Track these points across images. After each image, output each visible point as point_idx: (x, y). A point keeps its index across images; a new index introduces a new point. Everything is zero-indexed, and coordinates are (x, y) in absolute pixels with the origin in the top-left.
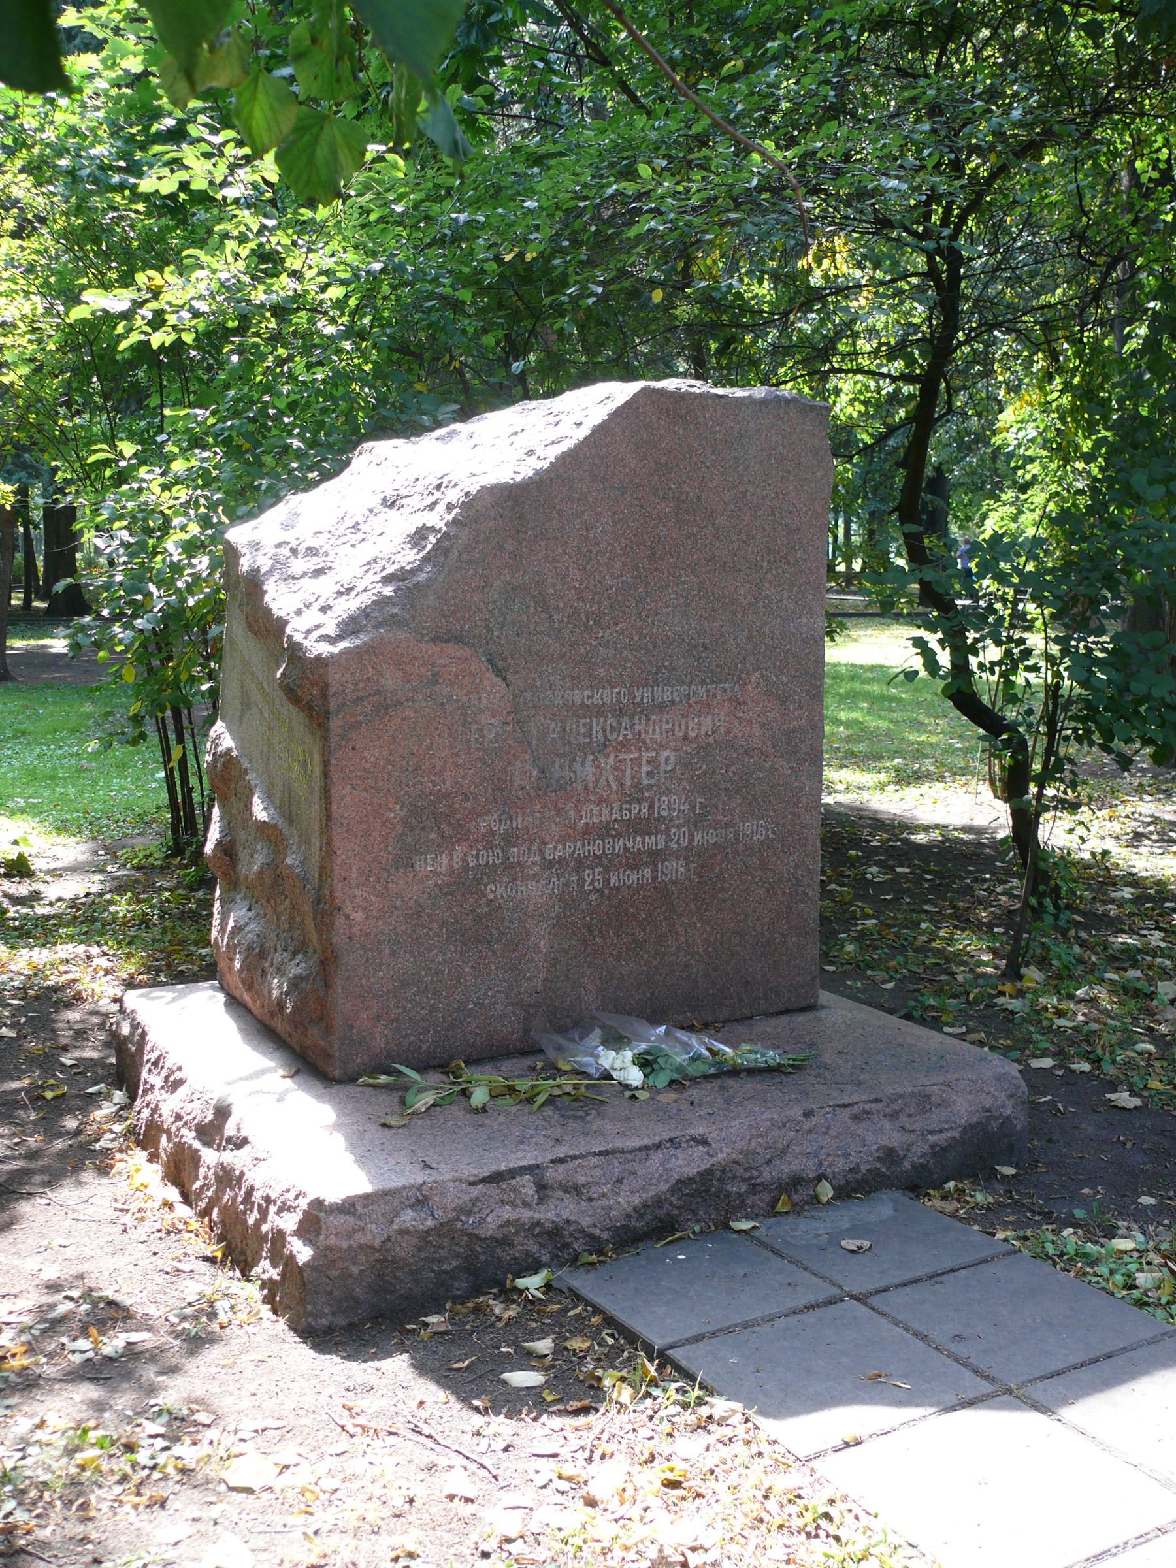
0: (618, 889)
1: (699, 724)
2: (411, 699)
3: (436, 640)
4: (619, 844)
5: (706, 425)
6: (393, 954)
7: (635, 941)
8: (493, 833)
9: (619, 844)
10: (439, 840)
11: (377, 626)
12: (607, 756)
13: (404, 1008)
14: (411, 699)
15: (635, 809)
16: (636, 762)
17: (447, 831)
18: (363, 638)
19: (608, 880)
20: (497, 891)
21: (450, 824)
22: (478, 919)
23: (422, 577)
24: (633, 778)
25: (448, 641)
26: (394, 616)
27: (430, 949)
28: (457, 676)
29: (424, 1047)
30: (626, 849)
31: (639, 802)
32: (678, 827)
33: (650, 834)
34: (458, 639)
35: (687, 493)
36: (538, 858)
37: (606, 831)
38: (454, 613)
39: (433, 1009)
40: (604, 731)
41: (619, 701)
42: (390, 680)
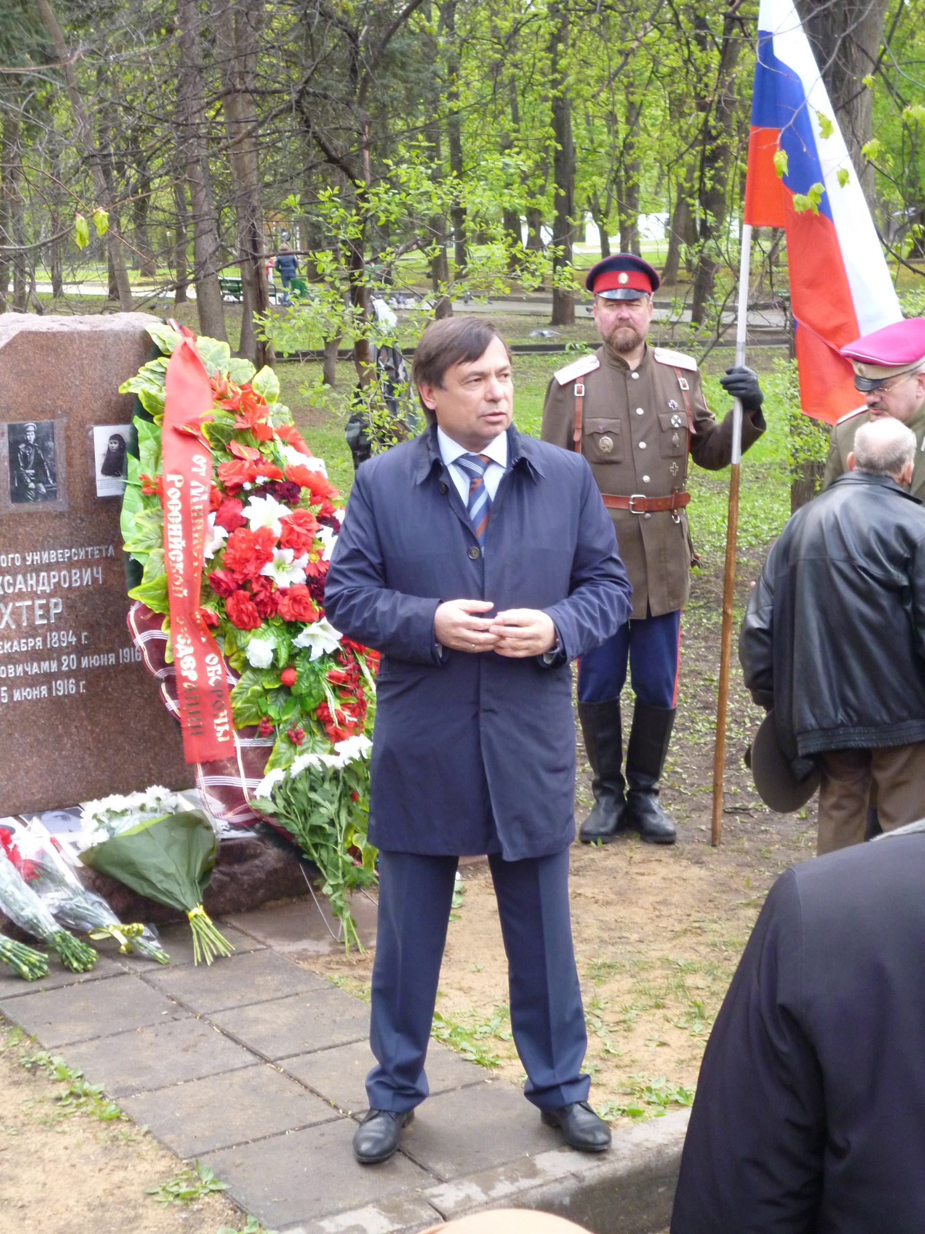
0: (20, 702)
1: (81, 577)
4: (20, 670)
7: (37, 740)
9: (20, 670)
12: (6, 606)
16: (31, 609)
19: (11, 697)
24: (28, 619)
30: (26, 672)
31: (34, 637)
33: (44, 660)
41: (13, 563)
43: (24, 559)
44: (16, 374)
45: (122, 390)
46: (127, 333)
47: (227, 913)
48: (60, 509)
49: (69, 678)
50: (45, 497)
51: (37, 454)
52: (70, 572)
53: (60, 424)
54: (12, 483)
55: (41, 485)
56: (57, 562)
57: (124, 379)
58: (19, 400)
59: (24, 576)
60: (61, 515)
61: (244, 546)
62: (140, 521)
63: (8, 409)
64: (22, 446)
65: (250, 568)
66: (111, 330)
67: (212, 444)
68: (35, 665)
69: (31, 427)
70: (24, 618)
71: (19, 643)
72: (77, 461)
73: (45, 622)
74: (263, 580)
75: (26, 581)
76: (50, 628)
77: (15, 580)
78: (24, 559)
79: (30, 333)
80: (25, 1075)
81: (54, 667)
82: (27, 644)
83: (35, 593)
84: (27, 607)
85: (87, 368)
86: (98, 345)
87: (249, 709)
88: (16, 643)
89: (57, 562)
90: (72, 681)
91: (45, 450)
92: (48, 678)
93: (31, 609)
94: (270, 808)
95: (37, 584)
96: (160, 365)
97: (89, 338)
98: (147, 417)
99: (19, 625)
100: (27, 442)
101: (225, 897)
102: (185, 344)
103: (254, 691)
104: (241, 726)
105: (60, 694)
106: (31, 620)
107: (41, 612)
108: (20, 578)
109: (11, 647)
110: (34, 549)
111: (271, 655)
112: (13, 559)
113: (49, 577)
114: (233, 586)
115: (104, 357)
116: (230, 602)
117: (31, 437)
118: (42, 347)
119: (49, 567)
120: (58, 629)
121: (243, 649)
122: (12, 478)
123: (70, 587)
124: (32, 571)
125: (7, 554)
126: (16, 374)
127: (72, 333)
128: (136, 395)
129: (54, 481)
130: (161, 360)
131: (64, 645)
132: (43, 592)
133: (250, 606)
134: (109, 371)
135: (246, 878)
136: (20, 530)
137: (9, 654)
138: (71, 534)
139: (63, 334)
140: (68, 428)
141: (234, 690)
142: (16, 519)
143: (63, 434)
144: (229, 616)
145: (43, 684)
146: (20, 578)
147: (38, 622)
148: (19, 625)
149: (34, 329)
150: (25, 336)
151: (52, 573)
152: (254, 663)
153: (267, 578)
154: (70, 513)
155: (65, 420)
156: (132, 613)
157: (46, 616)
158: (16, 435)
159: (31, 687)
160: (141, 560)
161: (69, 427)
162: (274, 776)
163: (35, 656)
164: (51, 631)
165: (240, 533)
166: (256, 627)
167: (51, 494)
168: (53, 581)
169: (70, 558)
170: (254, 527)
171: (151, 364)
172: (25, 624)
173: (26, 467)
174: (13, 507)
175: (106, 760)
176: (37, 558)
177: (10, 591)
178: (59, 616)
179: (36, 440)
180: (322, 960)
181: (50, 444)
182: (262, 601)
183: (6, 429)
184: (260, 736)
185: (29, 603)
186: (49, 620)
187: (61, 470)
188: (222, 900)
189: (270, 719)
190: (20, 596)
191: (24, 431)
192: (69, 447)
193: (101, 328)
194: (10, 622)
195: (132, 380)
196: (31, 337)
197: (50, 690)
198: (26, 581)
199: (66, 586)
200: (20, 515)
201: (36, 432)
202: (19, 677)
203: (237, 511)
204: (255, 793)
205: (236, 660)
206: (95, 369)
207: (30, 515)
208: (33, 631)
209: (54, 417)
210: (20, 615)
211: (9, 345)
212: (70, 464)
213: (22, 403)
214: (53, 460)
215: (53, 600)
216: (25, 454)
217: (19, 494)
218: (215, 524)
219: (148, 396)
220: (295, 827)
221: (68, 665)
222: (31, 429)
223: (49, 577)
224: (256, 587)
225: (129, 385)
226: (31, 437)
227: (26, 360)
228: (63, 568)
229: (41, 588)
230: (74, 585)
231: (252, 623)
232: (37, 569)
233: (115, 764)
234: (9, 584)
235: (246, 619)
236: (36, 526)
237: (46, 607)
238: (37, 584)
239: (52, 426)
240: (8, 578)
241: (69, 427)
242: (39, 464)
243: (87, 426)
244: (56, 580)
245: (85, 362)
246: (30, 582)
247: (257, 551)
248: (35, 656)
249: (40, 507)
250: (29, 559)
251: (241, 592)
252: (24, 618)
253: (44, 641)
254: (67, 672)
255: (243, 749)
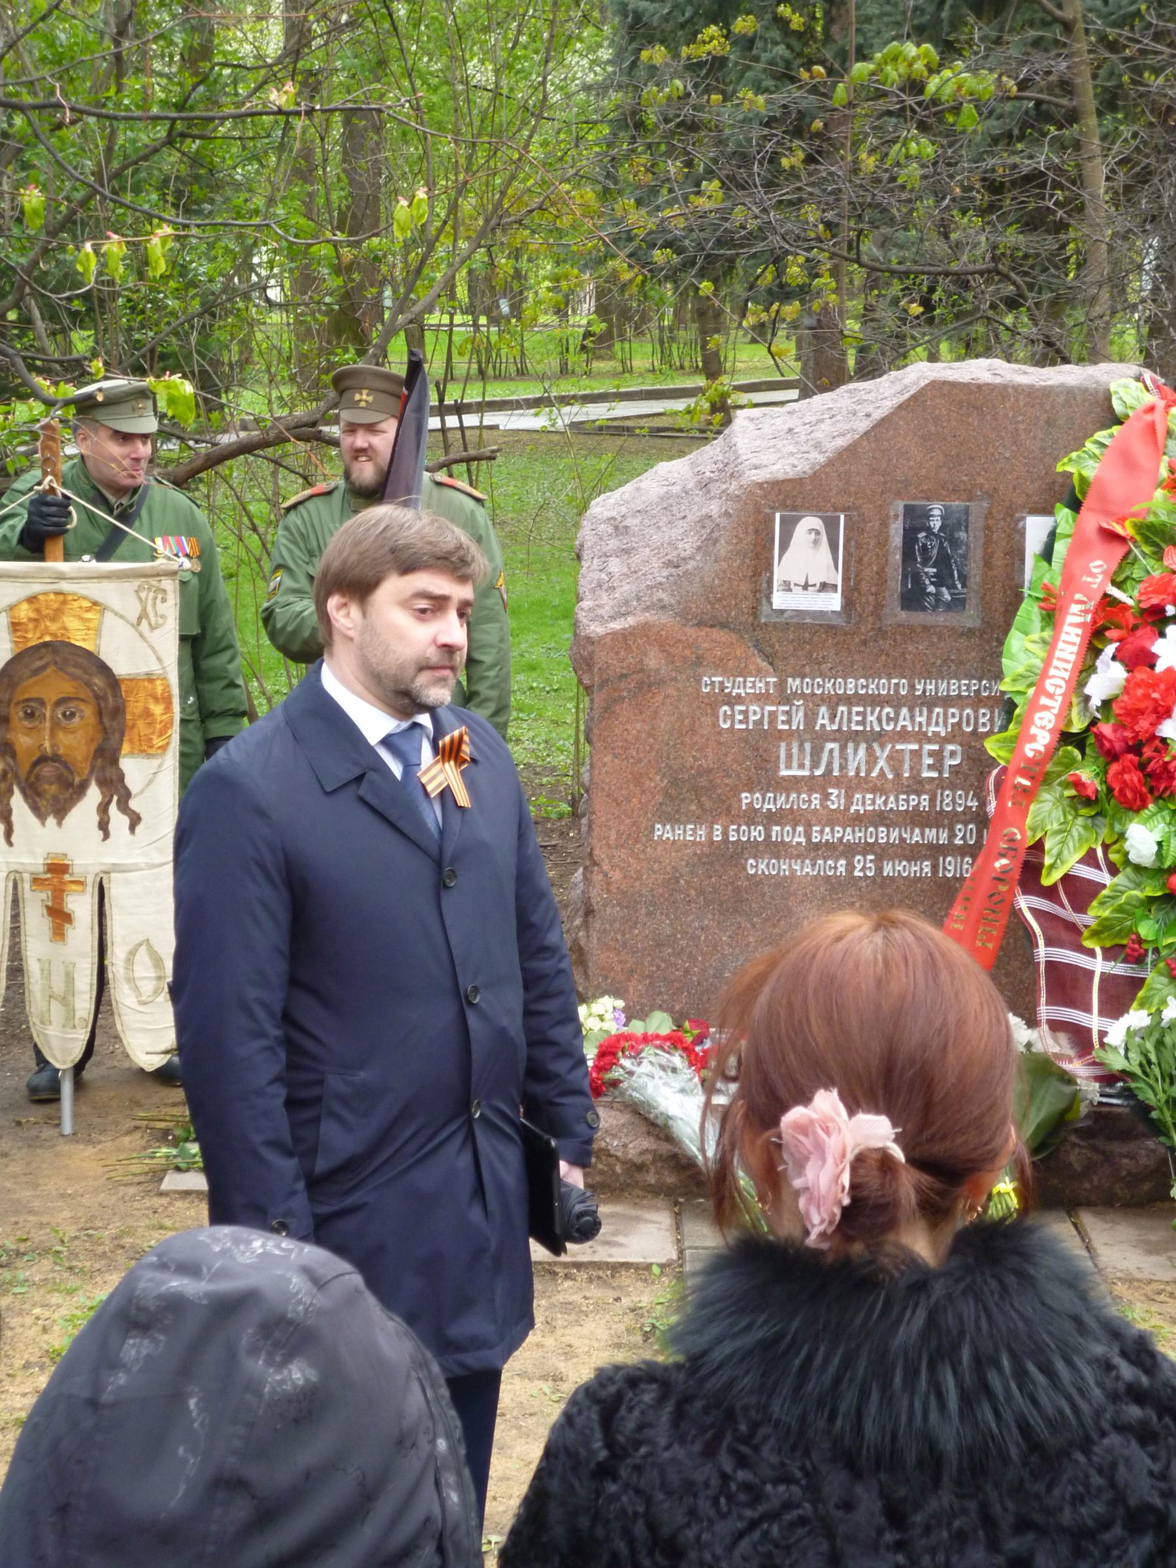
0: (892, 879)
2: (675, 679)
3: (699, 624)
5: (1006, 416)
6: (649, 914)
8: (756, 811)
9: (895, 835)
10: (699, 812)
11: (647, 609)
12: (882, 747)
13: (659, 967)
14: (675, 679)
15: (914, 800)
16: (916, 755)
17: (708, 804)
18: (631, 621)
19: (880, 869)
20: (757, 867)
21: (710, 798)
22: (737, 890)
23: (691, 565)
24: (911, 769)
25: (712, 626)
26: (660, 600)
27: (686, 914)
28: (721, 660)
29: (677, 1007)
31: (919, 795)
32: (966, 823)
33: (931, 827)
34: (723, 625)
35: (981, 486)
36: (802, 840)
37: (881, 818)
38: (720, 600)
39: (687, 972)
40: (879, 719)
42: (654, 660)
43: (912, 687)
44: (922, 437)
45: (1060, 468)
46: (1086, 390)
47: (1089, 1204)
48: (969, 624)
49: (963, 856)
50: (949, 607)
51: (941, 547)
52: (976, 712)
53: (978, 508)
54: (904, 584)
55: (944, 589)
56: (959, 696)
57: (1067, 453)
58: (923, 472)
59: (911, 710)
60: (970, 633)
61: (1140, 692)
62: (1031, 646)
63: (907, 484)
64: (922, 535)
65: (1143, 724)
66: (1062, 385)
67: (1147, 549)
68: (917, 831)
69: (937, 510)
70: (907, 766)
71: (897, 800)
72: (999, 561)
73: (935, 775)
74: (1157, 742)
75: (912, 718)
76: (941, 783)
77: (897, 714)
78: (912, 687)
79: (945, 382)
80: (638, 1338)
81: (943, 838)
82: (907, 801)
83: (925, 734)
84: (912, 751)
85: (1023, 436)
86: (1042, 405)
87: (1121, 921)
88: (892, 799)
89: (959, 696)
90: (968, 859)
91: (955, 543)
92: (934, 852)
93: (916, 755)
94: (1117, 1063)
95: (929, 724)
96: (1112, 436)
97: (1029, 395)
98: (1075, 505)
99: (898, 775)
100: (929, 530)
101: (1091, 1181)
102: (1151, 409)
103: (1132, 897)
104: (1108, 944)
105: (949, 875)
106: (915, 769)
107: (930, 761)
108: (904, 711)
109: (885, 803)
110: (929, 676)
111: (1156, 848)
112: (897, 685)
113: (945, 715)
114: (1118, 746)
115: (1050, 423)
116: (1115, 768)
117: (936, 524)
118: (961, 402)
119: (947, 702)
120: (953, 787)
121: (1122, 837)
122: (905, 577)
123: (975, 731)
124: (922, 704)
125: (889, 679)
126: (922, 437)
127: (1005, 387)
128: (1071, 474)
129: (964, 586)
130: (1115, 429)
131: (960, 809)
132: (936, 734)
133: (1133, 777)
134: (1055, 442)
135: (1125, 1161)
136: (910, 648)
137: (882, 812)
138: (983, 660)
139: (991, 387)
140: (989, 515)
141: (1105, 892)
142: (908, 633)
143: (981, 523)
144: (1110, 790)
145: (925, 858)
146: (904, 711)
147: (926, 774)
148: (898, 775)
149: (951, 379)
150: (938, 387)
151: (952, 710)
152: (1132, 857)
153: (1164, 740)
154: (983, 631)
155: (985, 505)
156: (995, 772)
157: (937, 766)
158: (915, 520)
159: (909, 861)
160: (1017, 700)
161: (990, 513)
162: (1137, 1018)
163: (917, 819)
164: (943, 789)
165: (1141, 674)
166: (1144, 806)
167: (958, 603)
168: (951, 721)
169: (978, 692)
170: (1160, 667)
171: (1101, 436)
172: (906, 775)
173: (925, 563)
174: (903, 615)
175: (1007, 974)
176: (931, 687)
177: (890, 728)
178: (955, 770)
179: (941, 529)
180: (1155, 1286)
181: (962, 535)
182: (1154, 771)
183: (901, 510)
184: (1125, 961)
185: (915, 747)
186: (940, 772)
187: (973, 572)
188: (1087, 1185)
189: (1140, 941)
190: (903, 735)
191: (927, 515)
192: (988, 541)
193: (1049, 383)
194: (886, 770)
195: (1074, 455)
196: (945, 389)
197: (935, 868)
198: (912, 718)
199: (969, 729)
200: (912, 629)
201: (943, 518)
202: (893, 845)
203: (1146, 643)
204: (1106, 1040)
205: (1118, 852)
206: (1034, 438)
207: (926, 628)
208: (917, 785)
209: (970, 500)
210: (902, 762)
211: (914, 398)
212: (988, 564)
213: (926, 477)
214: (964, 556)
215: (951, 747)
216: (924, 546)
217: (913, 598)
218: (1114, 658)
219: (1083, 479)
220: (1151, 1095)
221: (964, 838)
222: (937, 512)
223: (945, 715)
224: (1148, 752)
225: (1070, 460)
226: (936, 524)
227: (937, 420)
228: (967, 706)
229: (933, 728)
230: (981, 730)
231: (1138, 803)
232: (930, 702)
233: (1022, 981)
234: (889, 719)
235: (1129, 795)
236: (932, 644)
237: (938, 756)
238: (929, 724)
239: (967, 510)
240: (887, 710)
241: (990, 513)
242: (943, 561)
243: (1017, 515)
244: (956, 720)
245: (1022, 427)
246: (918, 719)
247: (1155, 700)
248: (917, 819)
249: (940, 619)
250: (920, 687)
251: (1130, 756)
252: (907, 766)
253: (932, 800)
254: (960, 847)
255: (1103, 974)
